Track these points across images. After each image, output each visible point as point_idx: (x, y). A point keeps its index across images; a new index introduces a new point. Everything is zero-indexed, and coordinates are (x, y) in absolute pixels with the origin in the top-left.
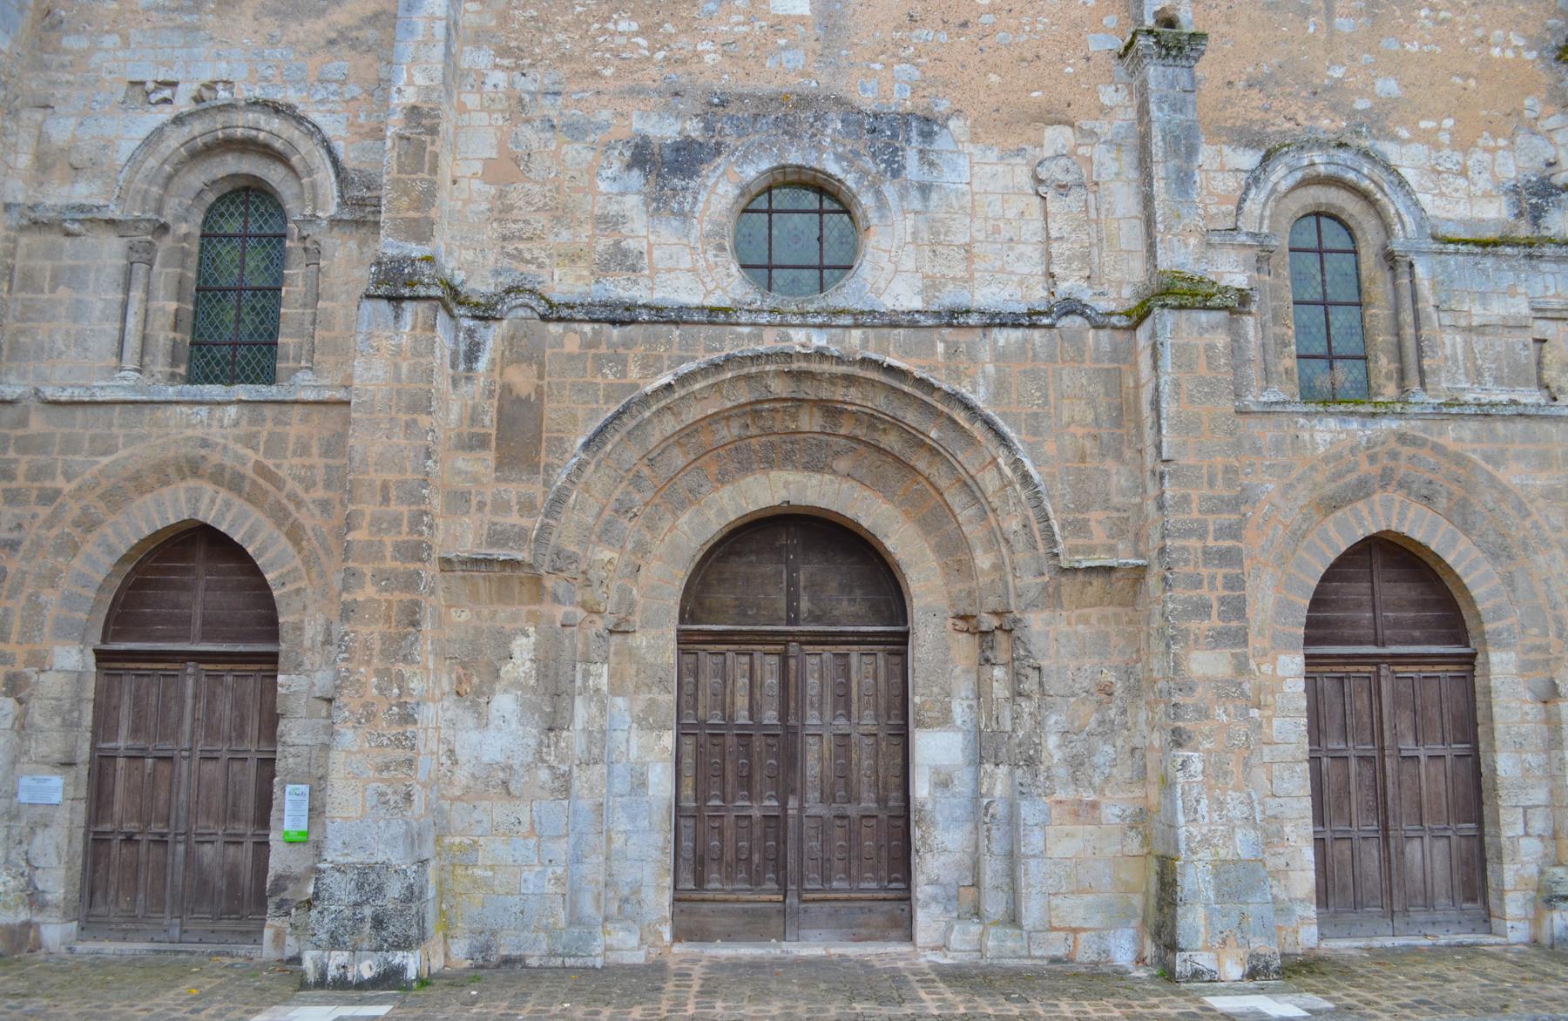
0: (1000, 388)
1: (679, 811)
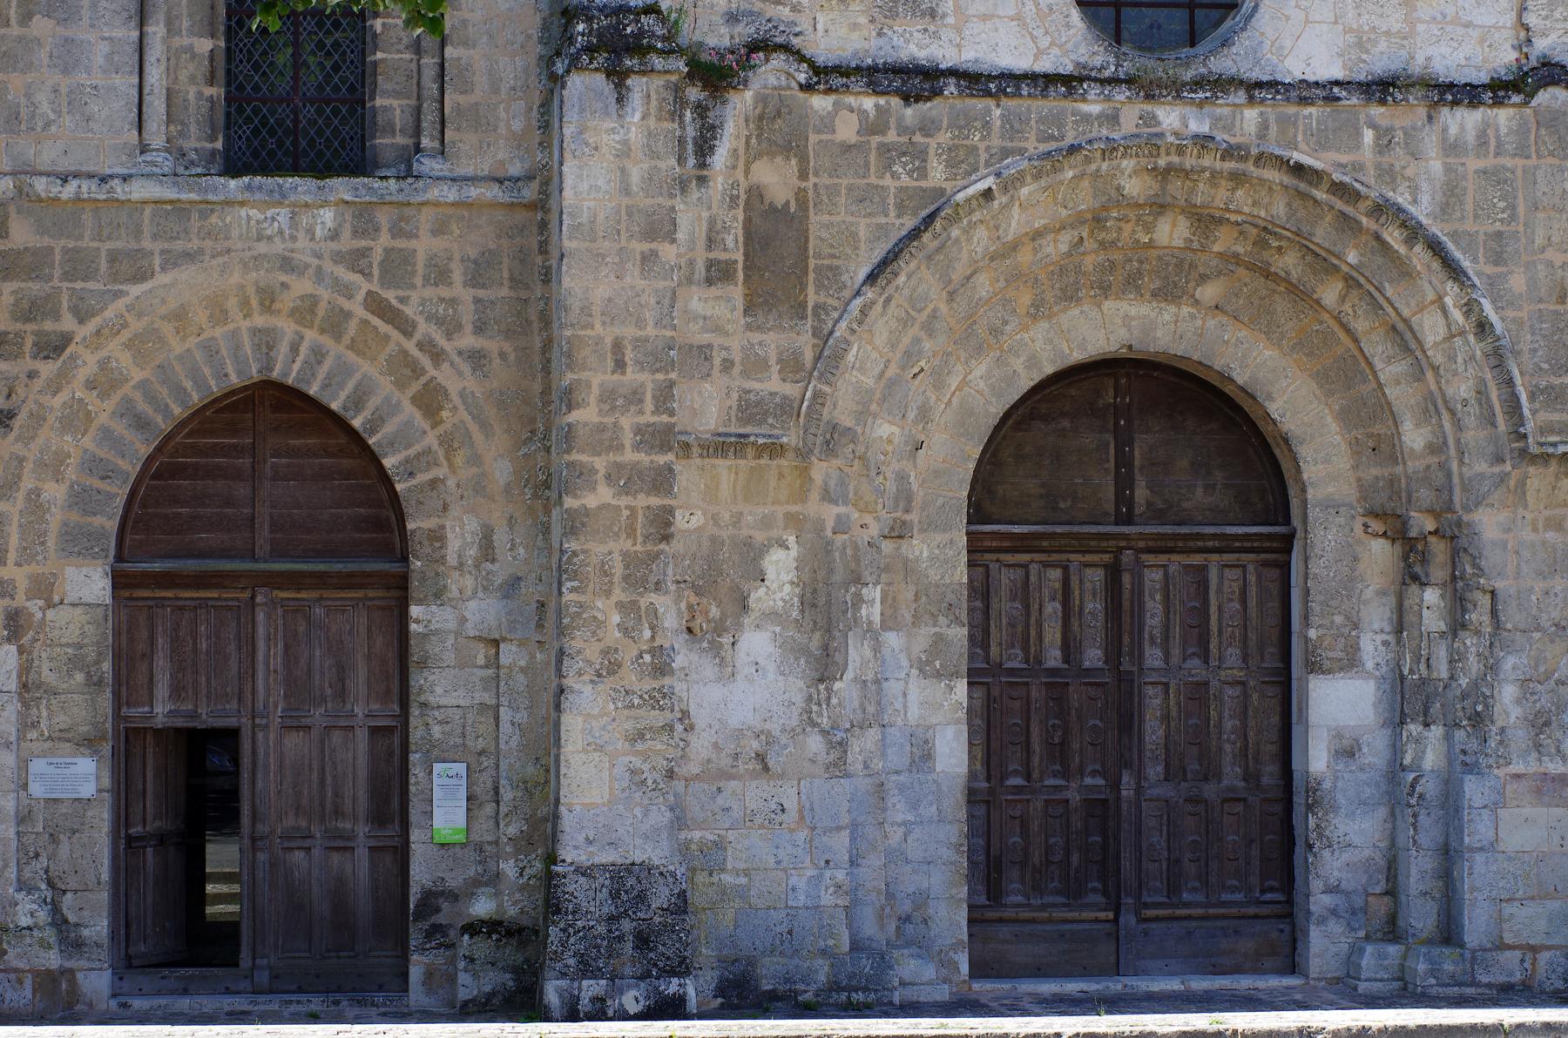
1: (972, 797)
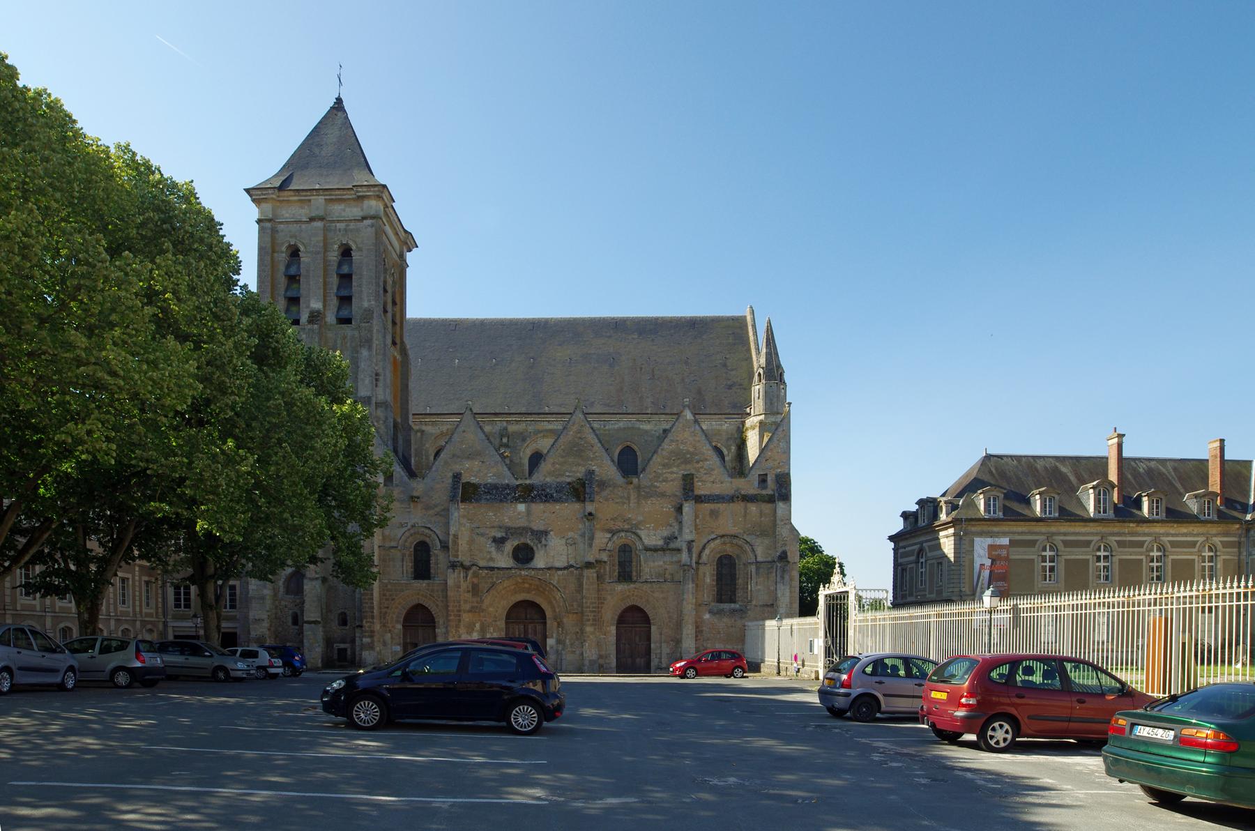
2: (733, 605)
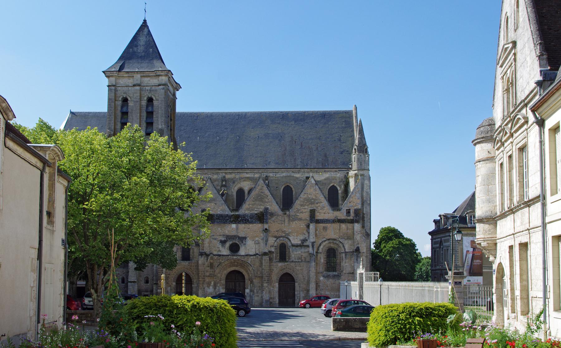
0: (251, 262)
2: (334, 273)
